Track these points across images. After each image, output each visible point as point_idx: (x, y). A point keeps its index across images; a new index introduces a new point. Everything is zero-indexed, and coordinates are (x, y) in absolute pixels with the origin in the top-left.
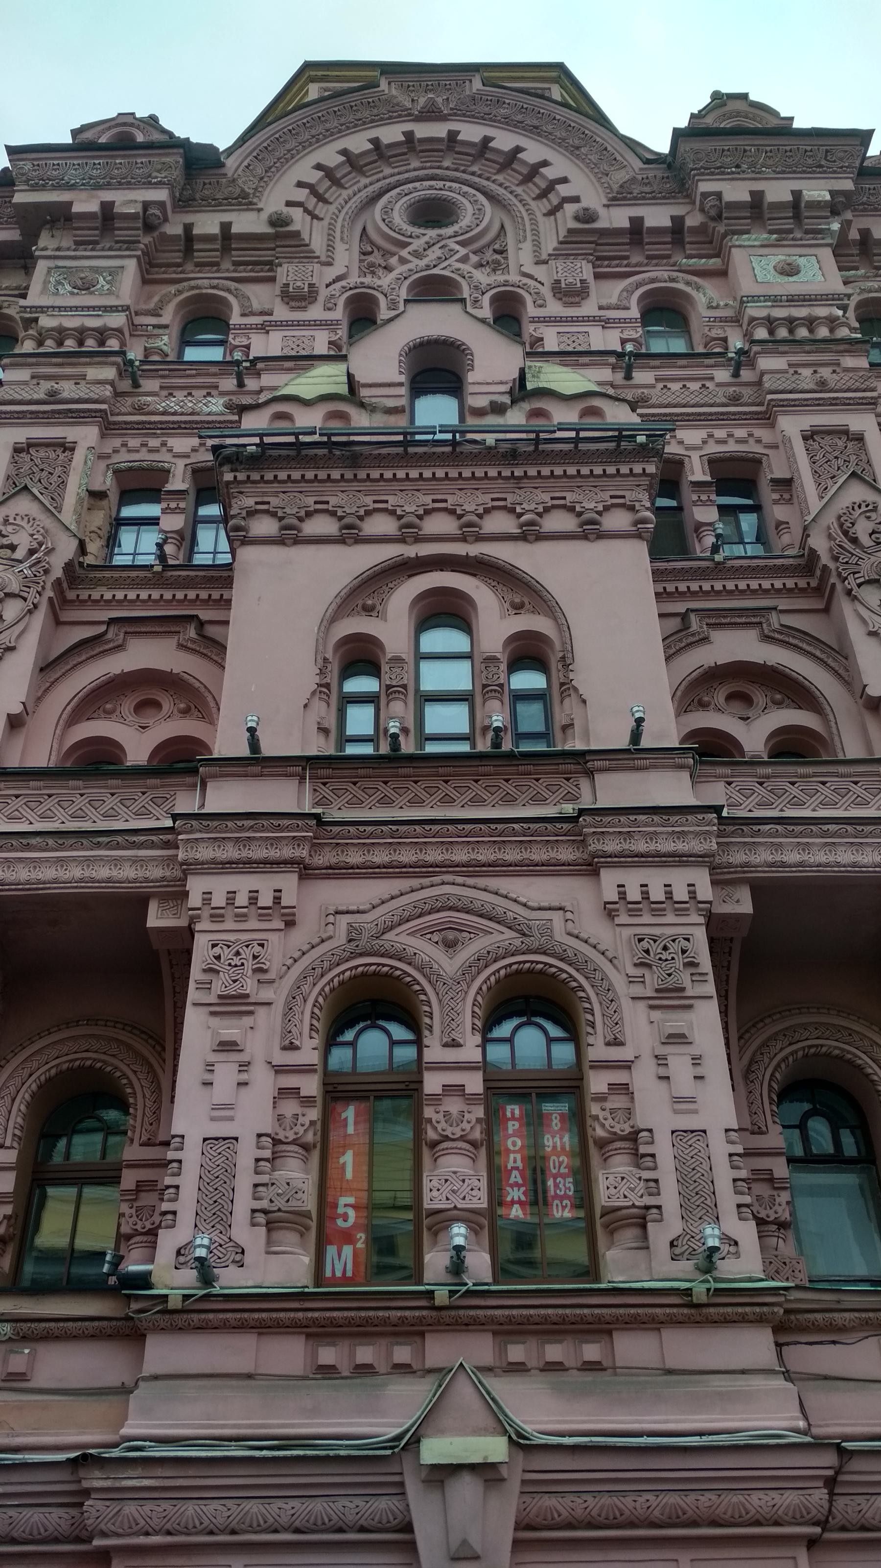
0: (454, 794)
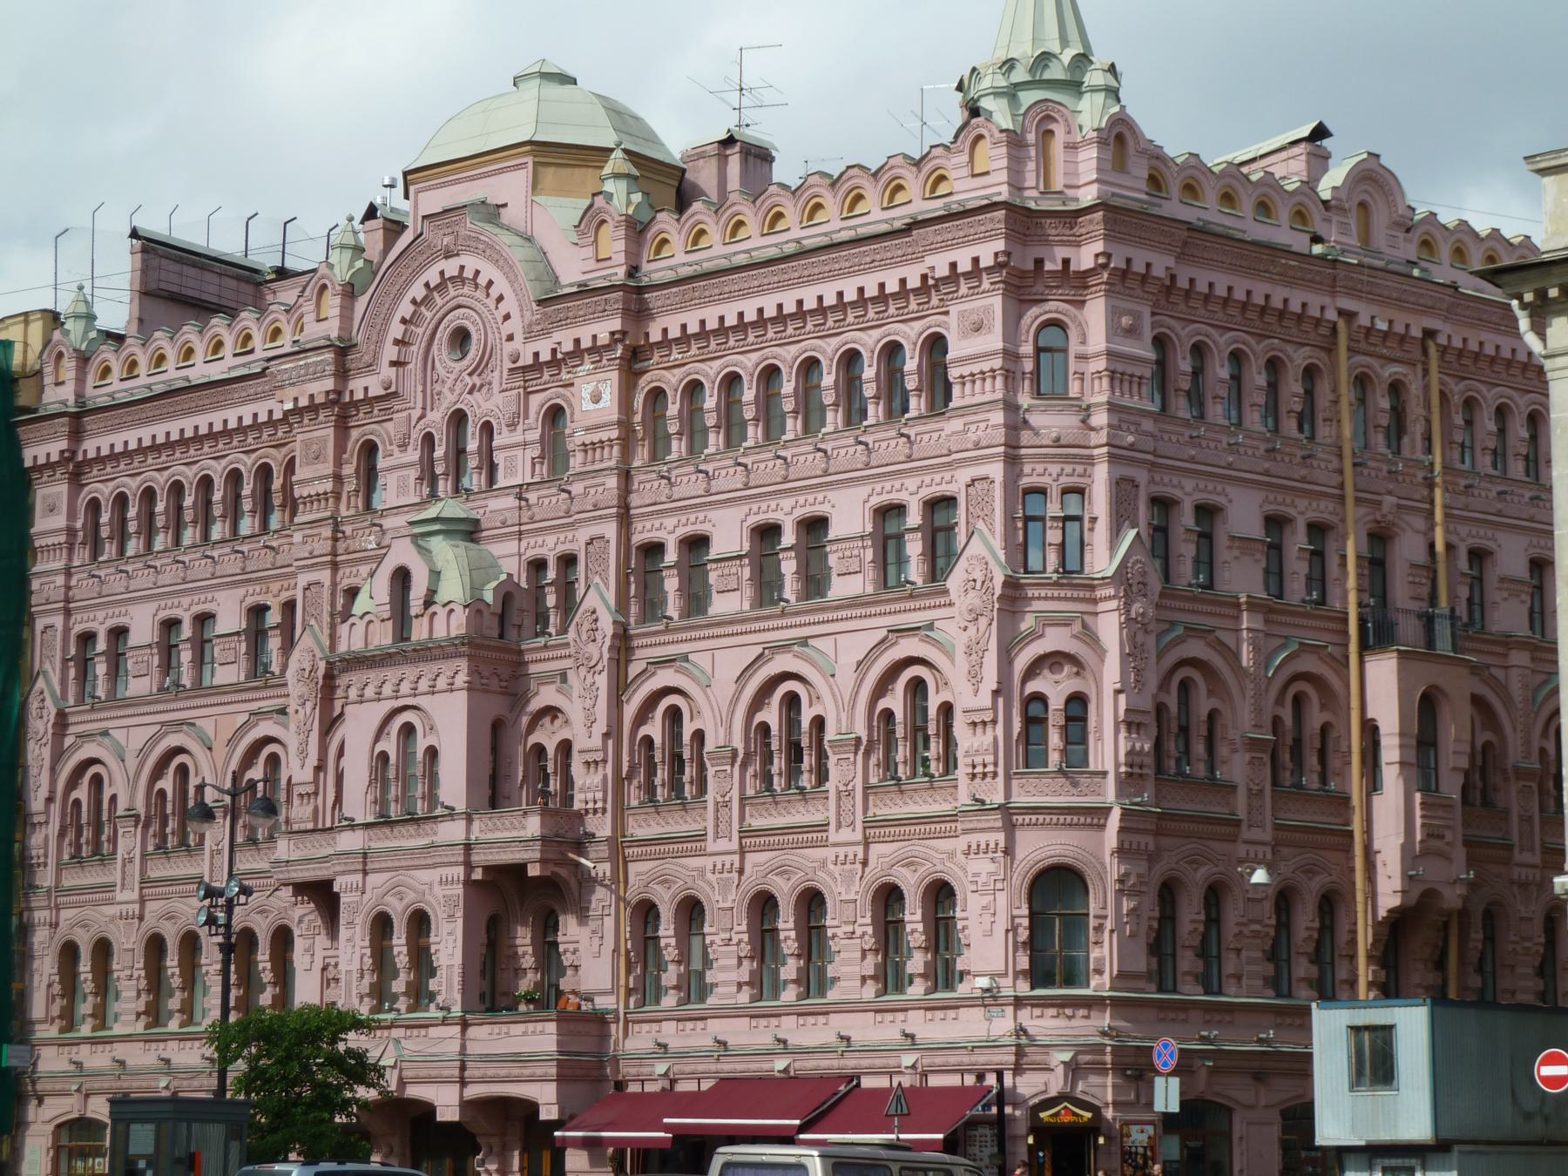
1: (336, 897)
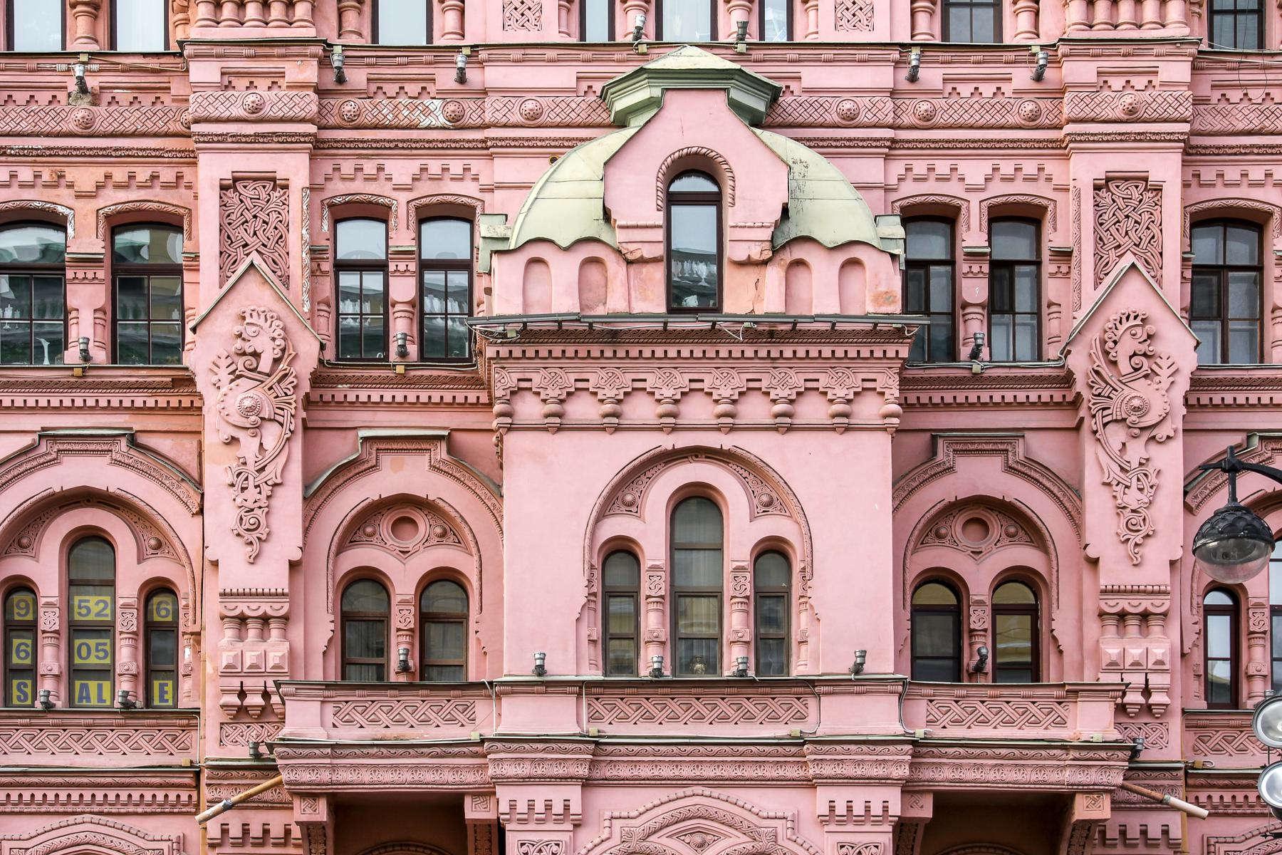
0: (705, 711)
1: (496, 832)
